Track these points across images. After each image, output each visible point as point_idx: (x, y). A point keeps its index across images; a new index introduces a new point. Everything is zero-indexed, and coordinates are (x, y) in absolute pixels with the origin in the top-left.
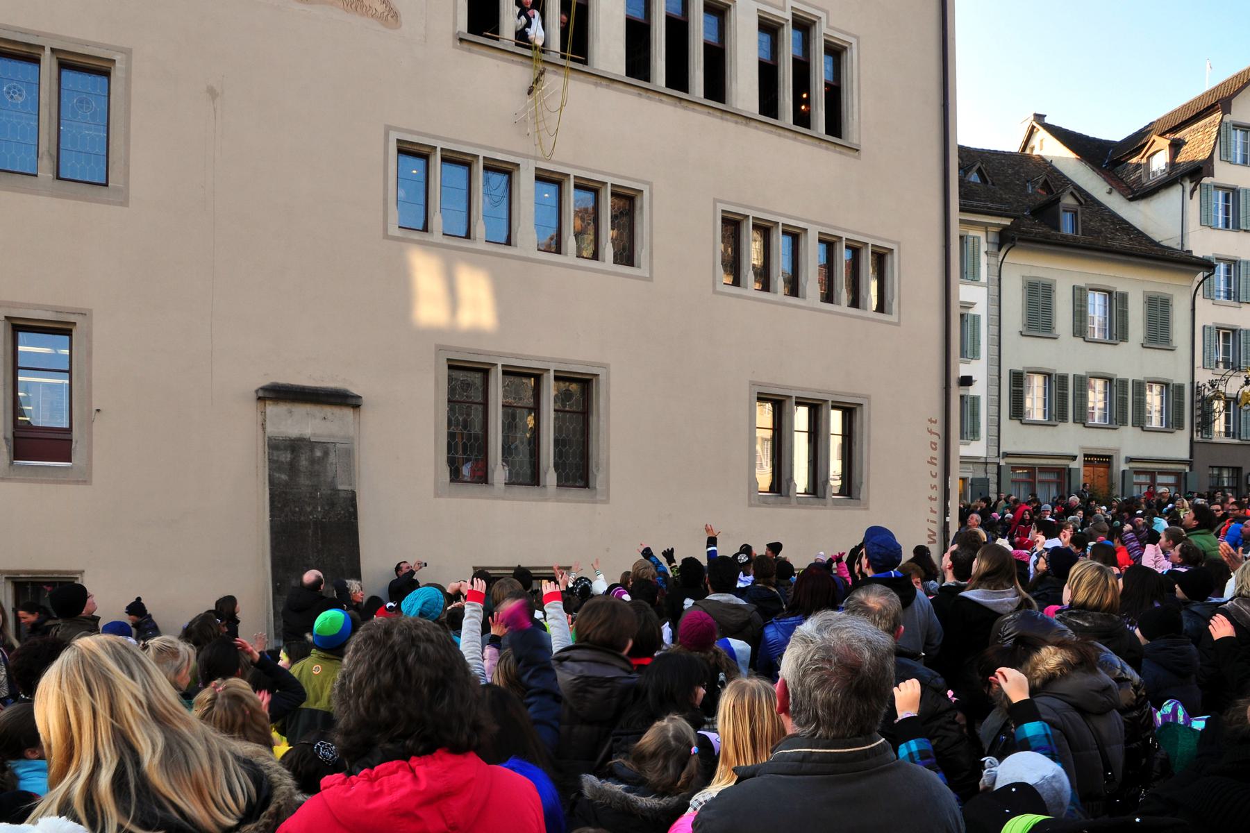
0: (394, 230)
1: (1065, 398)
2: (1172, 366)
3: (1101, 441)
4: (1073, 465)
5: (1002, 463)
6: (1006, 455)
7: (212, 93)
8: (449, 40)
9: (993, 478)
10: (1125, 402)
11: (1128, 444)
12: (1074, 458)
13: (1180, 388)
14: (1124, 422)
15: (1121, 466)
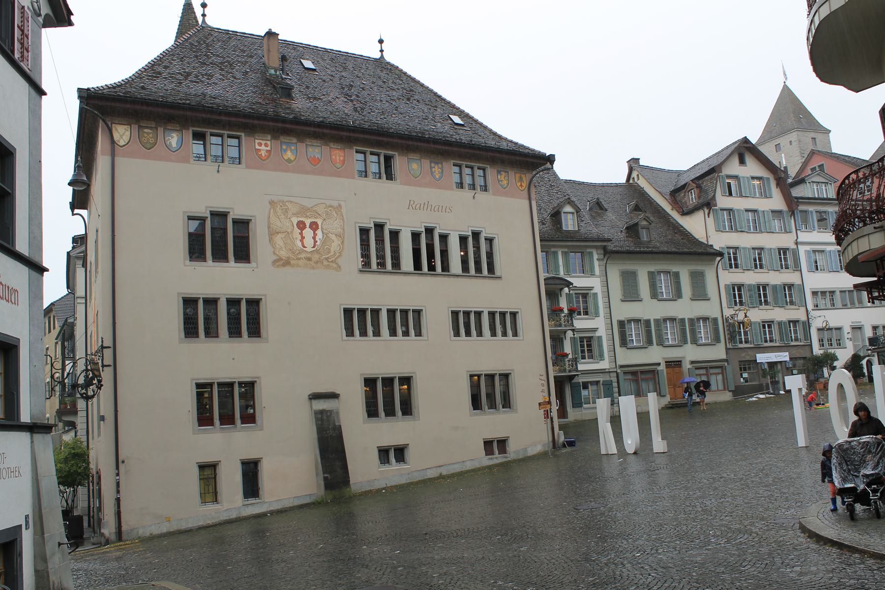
0: (345, 337)
1: (652, 333)
2: (710, 309)
3: (674, 354)
4: (660, 368)
5: (619, 371)
6: (621, 367)
7: (289, 303)
8: (356, 271)
9: (614, 379)
10: (688, 330)
11: (690, 354)
12: (659, 364)
13: (715, 320)
14: (686, 342)
15: (687, 366)
